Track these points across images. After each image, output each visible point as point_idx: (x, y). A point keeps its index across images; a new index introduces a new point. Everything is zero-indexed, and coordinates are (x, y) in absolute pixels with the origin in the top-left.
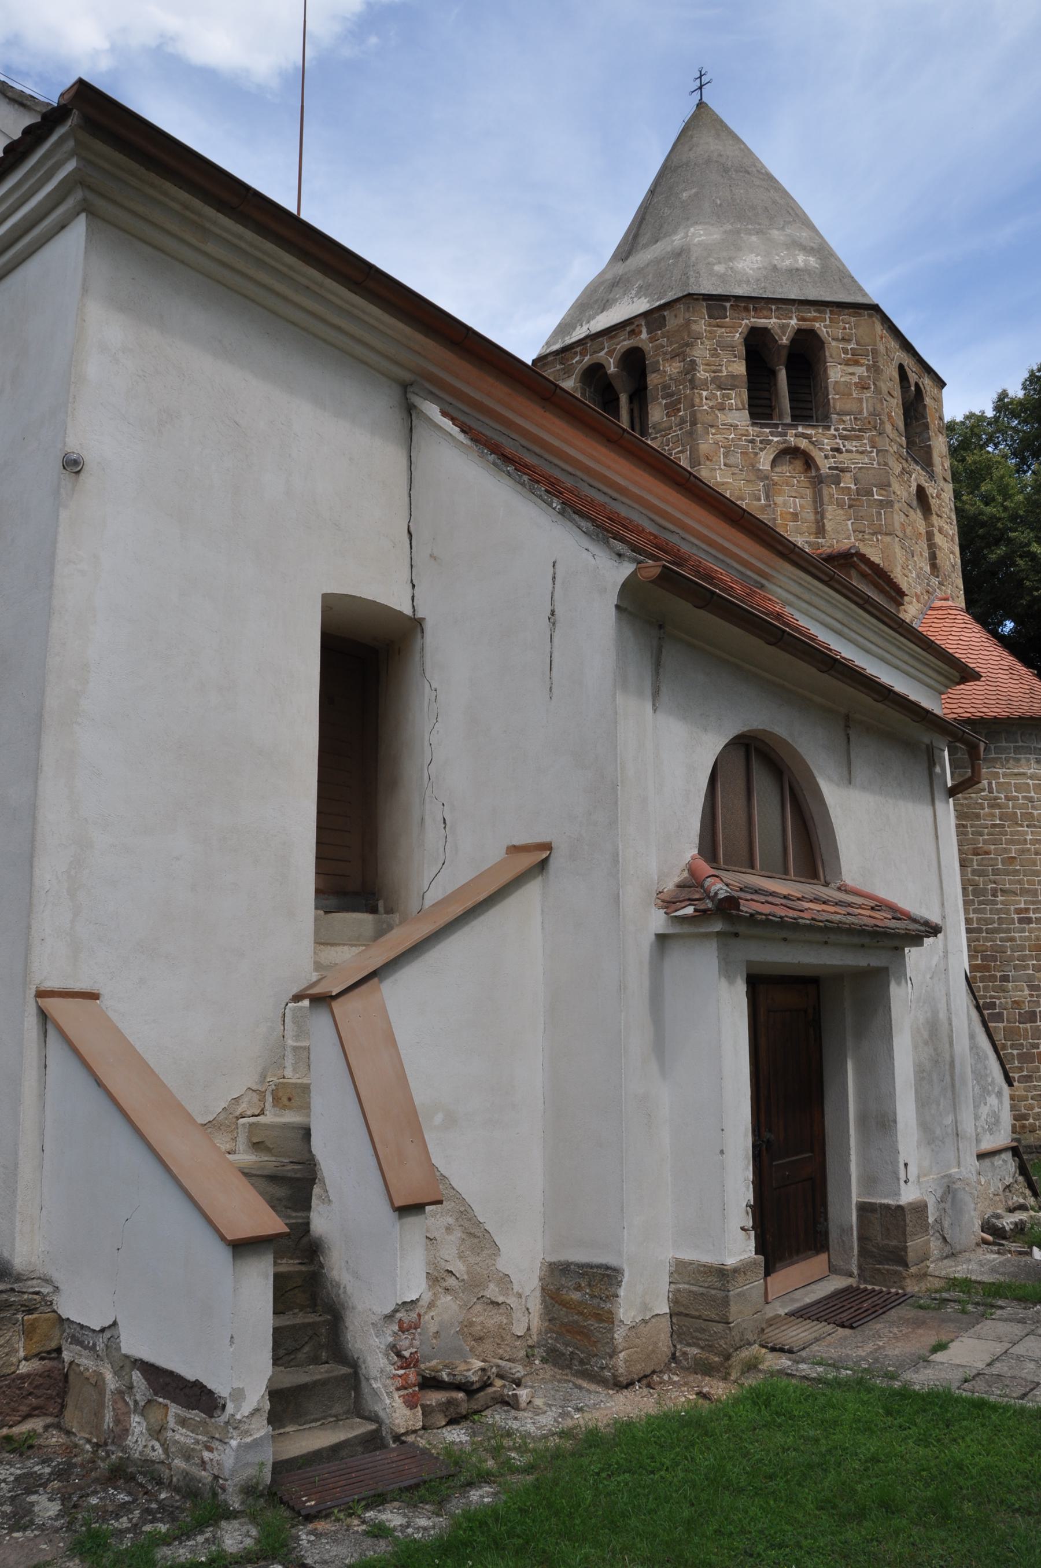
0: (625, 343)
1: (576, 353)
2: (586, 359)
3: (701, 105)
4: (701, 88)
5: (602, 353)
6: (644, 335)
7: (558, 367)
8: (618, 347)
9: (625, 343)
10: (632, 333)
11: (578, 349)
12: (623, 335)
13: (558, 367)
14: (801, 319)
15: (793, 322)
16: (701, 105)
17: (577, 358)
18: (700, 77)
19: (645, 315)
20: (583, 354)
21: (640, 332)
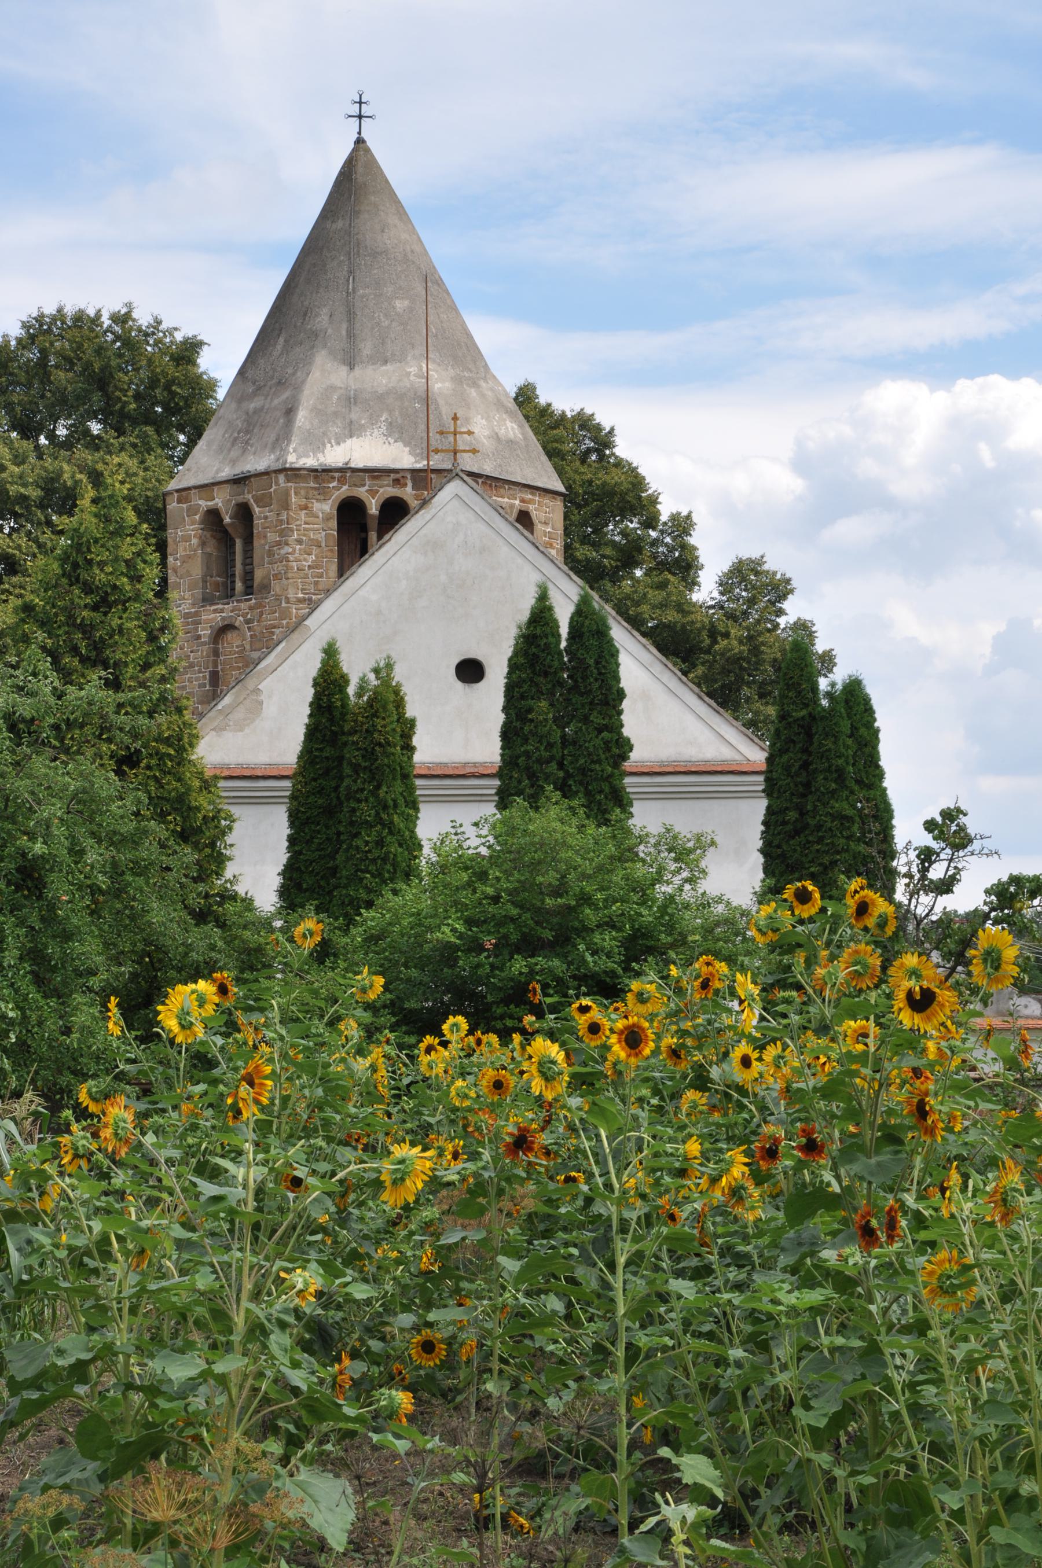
0: (390, 489)
1: (333, 478)
2: (345, 488)
3: (360, 141)
4: (360, 117)
5: (363, 489)
6: (409, 489)
7: (312, 484)
8: (381, 490)
9: (389, 491)
10: (397, 482)
11: (336, 475)
12: (388, 480)
13: (312, 484)
14: (523, 501)
15: (517, 502)
16: (360, 141)
17: (335, 484)
18: (360, 103)
19: (413, 471)
20: (342, 481)
21: (406, 485)
